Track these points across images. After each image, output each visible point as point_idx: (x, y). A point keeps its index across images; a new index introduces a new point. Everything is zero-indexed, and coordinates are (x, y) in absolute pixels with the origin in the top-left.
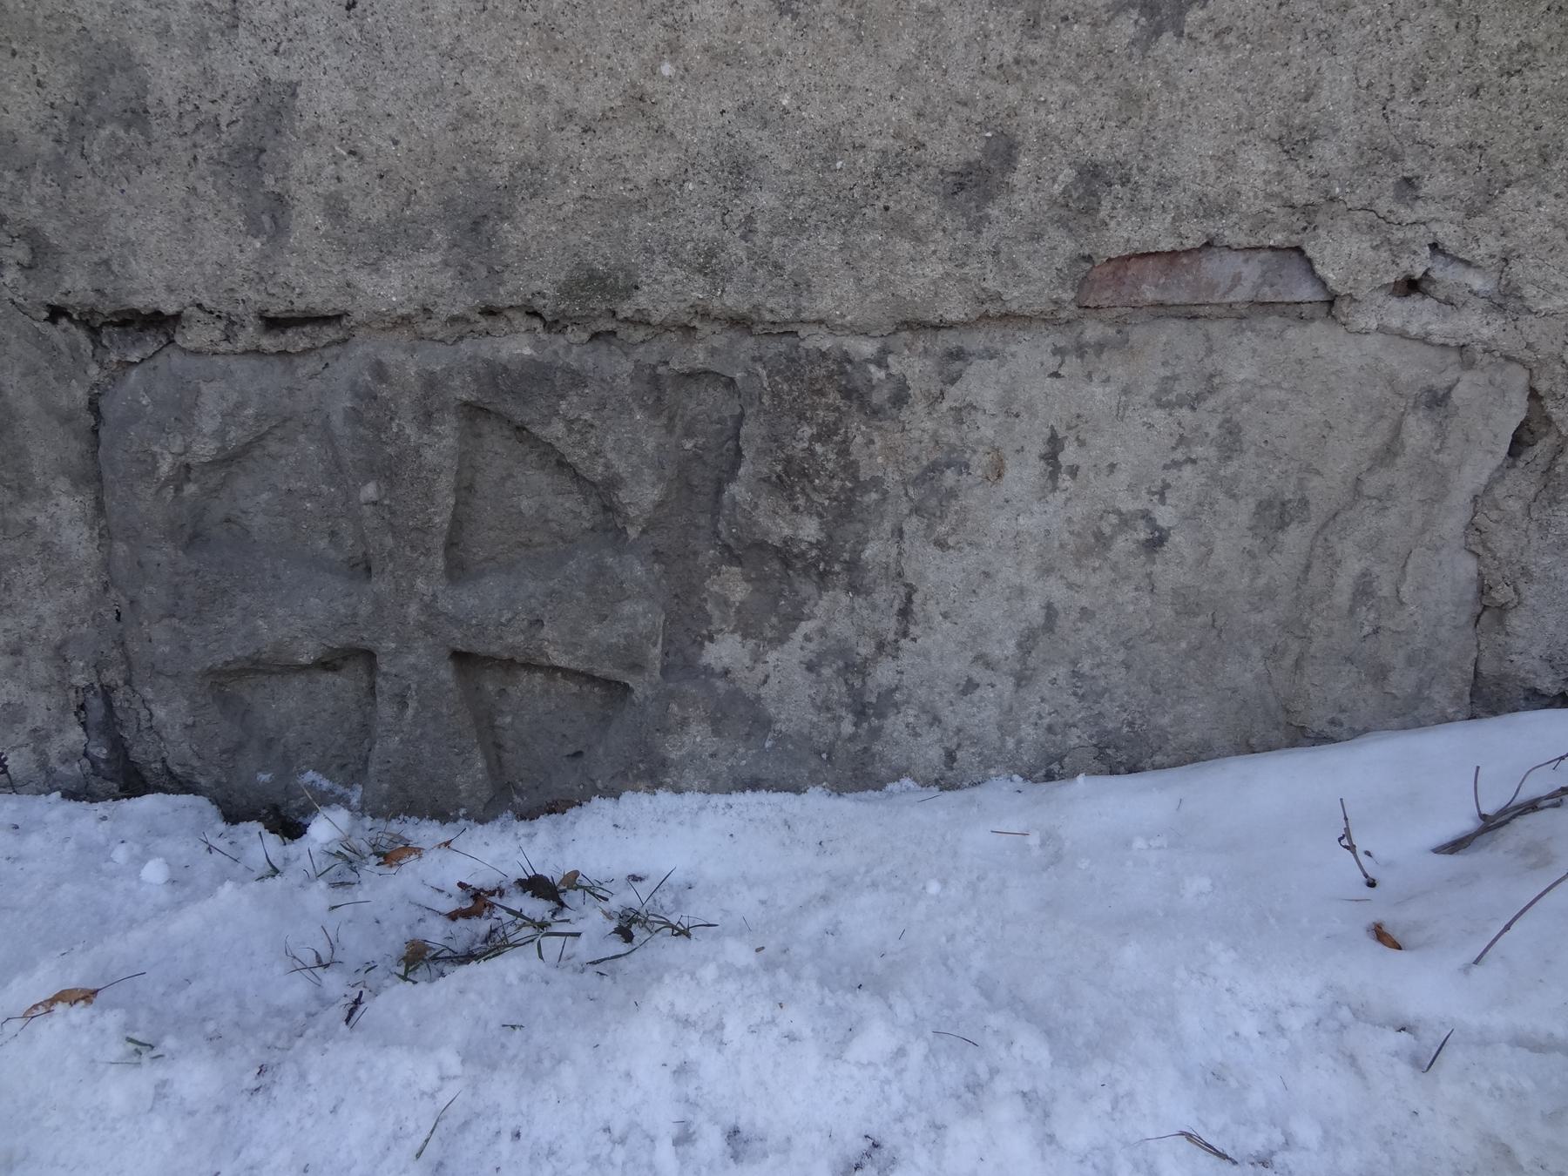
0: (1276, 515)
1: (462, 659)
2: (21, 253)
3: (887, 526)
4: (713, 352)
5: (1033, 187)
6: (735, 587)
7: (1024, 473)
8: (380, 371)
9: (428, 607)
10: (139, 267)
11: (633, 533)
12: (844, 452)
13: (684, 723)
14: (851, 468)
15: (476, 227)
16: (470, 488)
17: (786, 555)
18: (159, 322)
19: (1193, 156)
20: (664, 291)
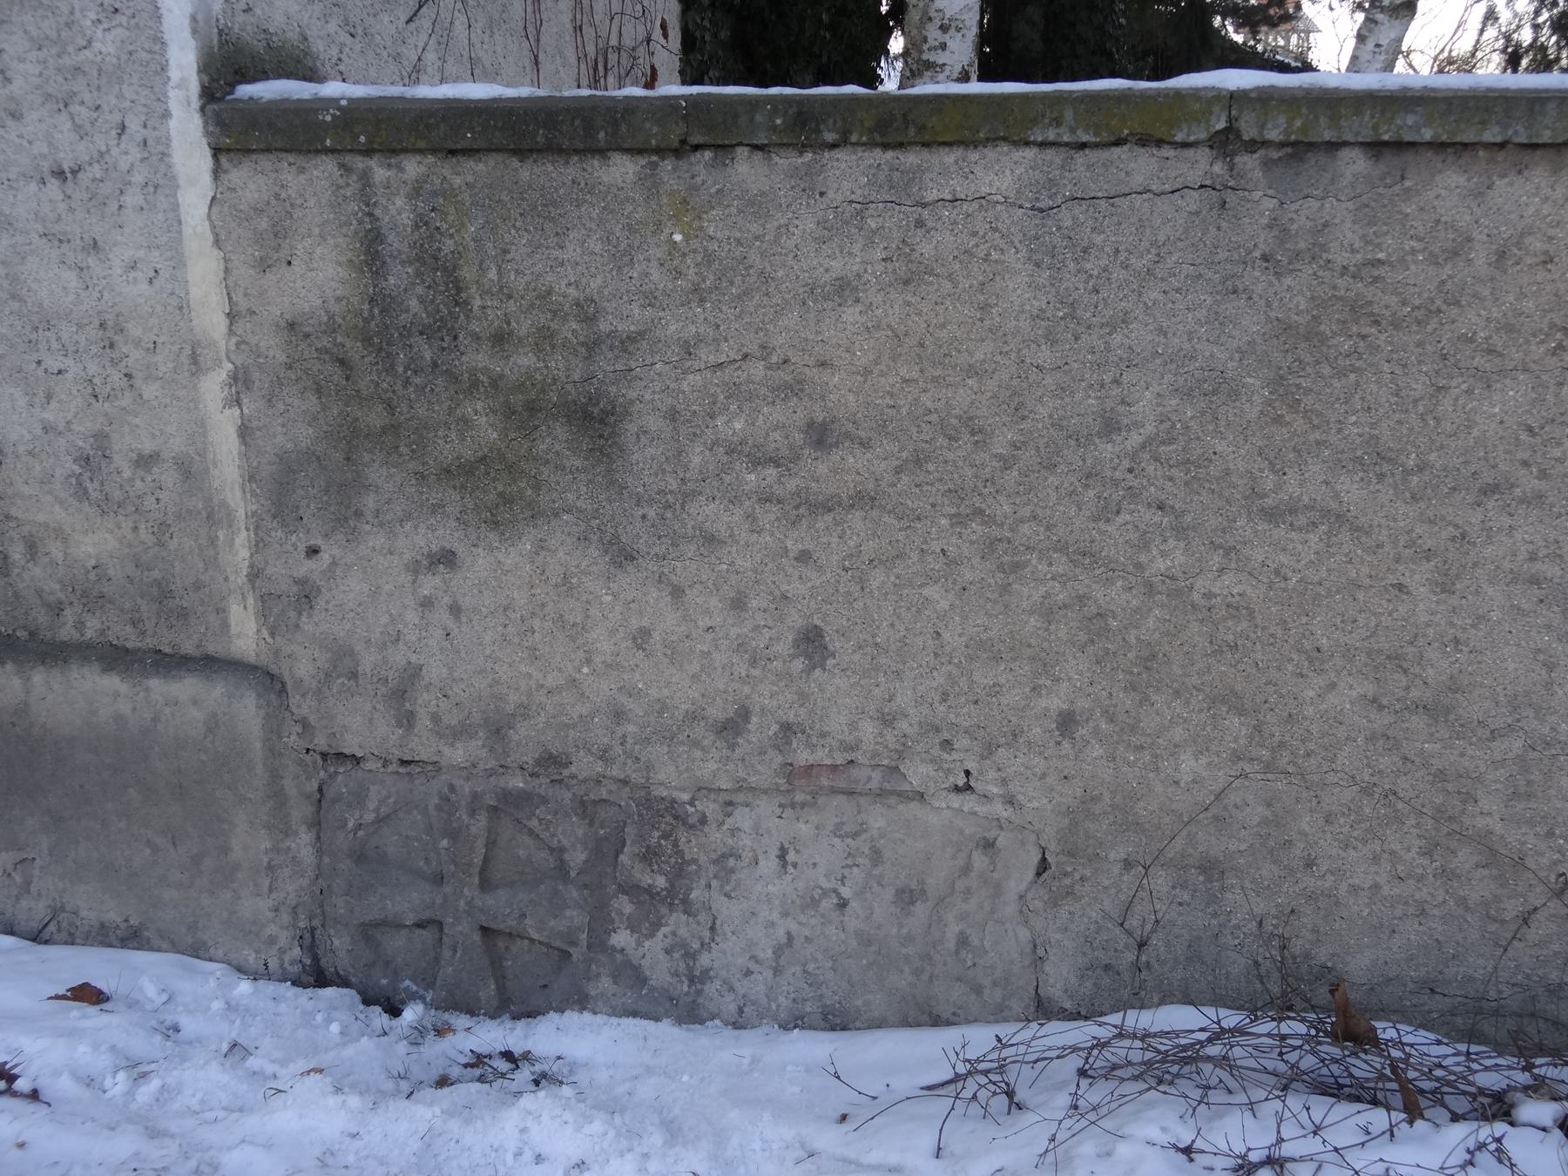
0: (907, 897)
1: (485, 930)
2: (299, 729)
3: (703, 882)
4: (610, 792)
5: (758, 731)
6: (625, 905)
7: (769, 864)
8: (452, 788)
9: (470, 903)
10: (348, 737)
11: (573, 874)
12: (675, 845)
13: (598, 975)
14: (680, 853)
15: (498, 731)
16: (494, 842)
17: (650, 891)
18: (356, 760)
19: (837, 723)
20: (585, 765)
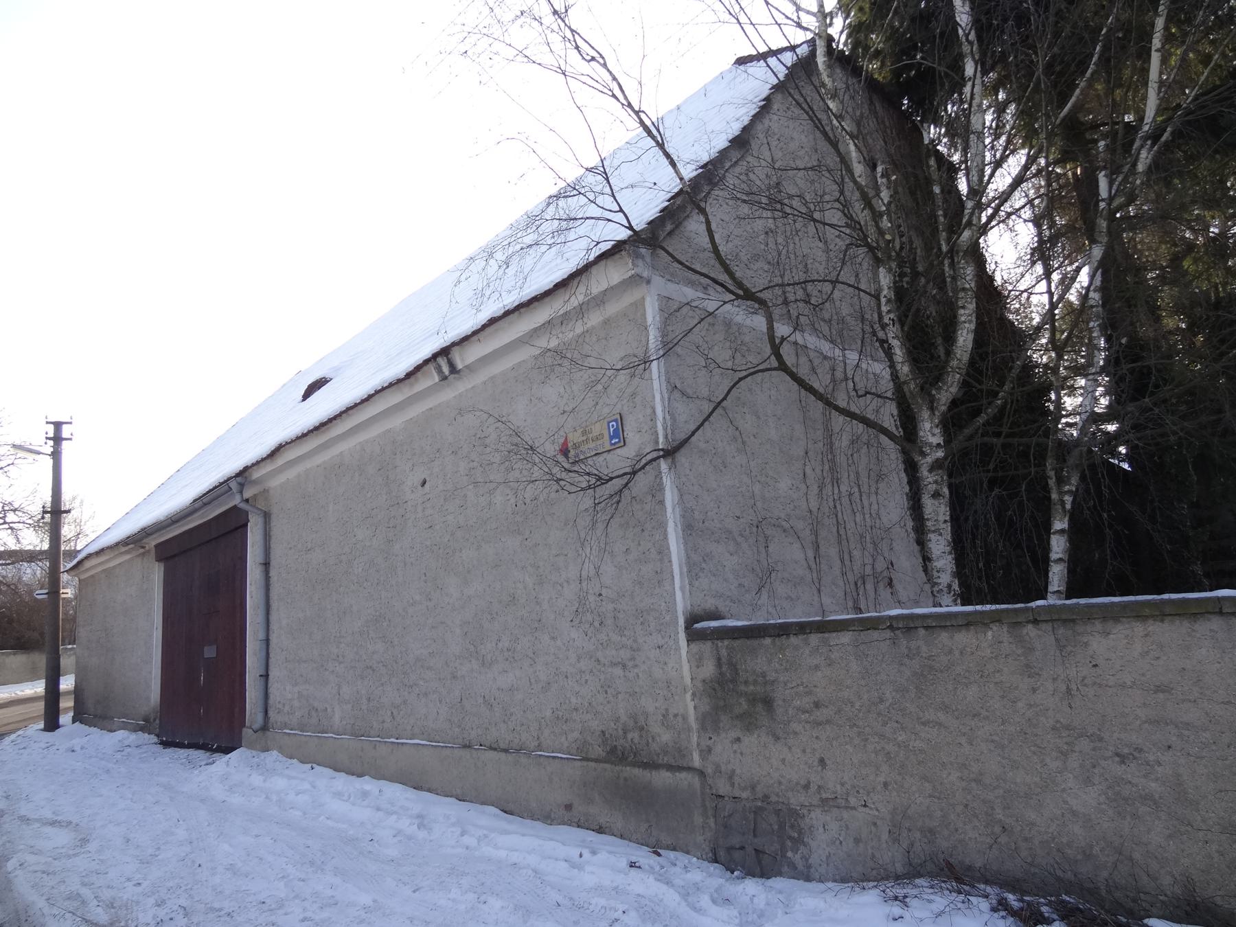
0: (857, 841)
5: (813, 788)
7: (821, 830)
15: (753, 788)
19: (831, 785)
20: (774, 799)
